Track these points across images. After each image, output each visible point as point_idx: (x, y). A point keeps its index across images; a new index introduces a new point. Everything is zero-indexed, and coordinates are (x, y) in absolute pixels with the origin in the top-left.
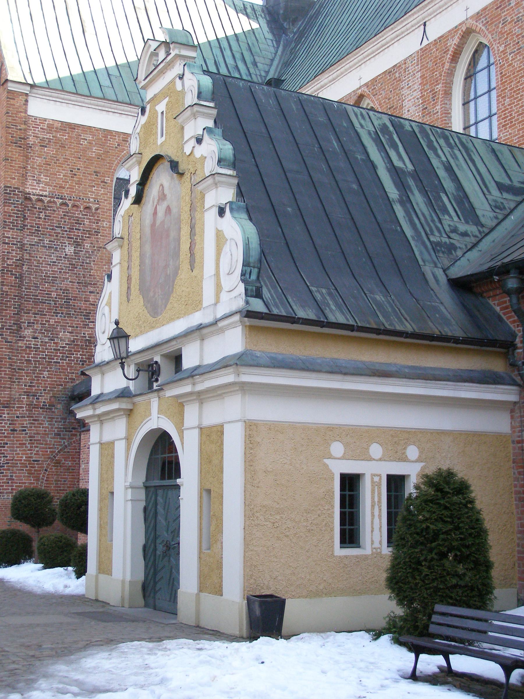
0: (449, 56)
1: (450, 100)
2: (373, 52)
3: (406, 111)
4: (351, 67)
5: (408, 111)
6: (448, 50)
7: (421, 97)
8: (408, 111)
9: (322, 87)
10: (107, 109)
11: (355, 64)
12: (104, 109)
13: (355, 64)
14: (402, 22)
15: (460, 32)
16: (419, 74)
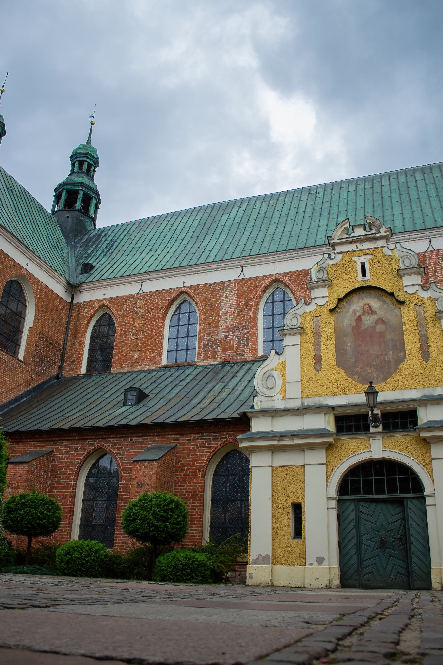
0: (261, 288)
1: (258, 311)
2: (198, 271)
3: (223, 309)
4: (177, 274)
5: (225, 309)
6: (261, 286)
7: (236, 304)
8: (225, 309)
9: (148, 279)
10: (10, 241)
11: (181, 274)
12: (8, 240)
13: (181, 274)
14: (227, 262)
15: (270, 278)
16: (236, 292)
